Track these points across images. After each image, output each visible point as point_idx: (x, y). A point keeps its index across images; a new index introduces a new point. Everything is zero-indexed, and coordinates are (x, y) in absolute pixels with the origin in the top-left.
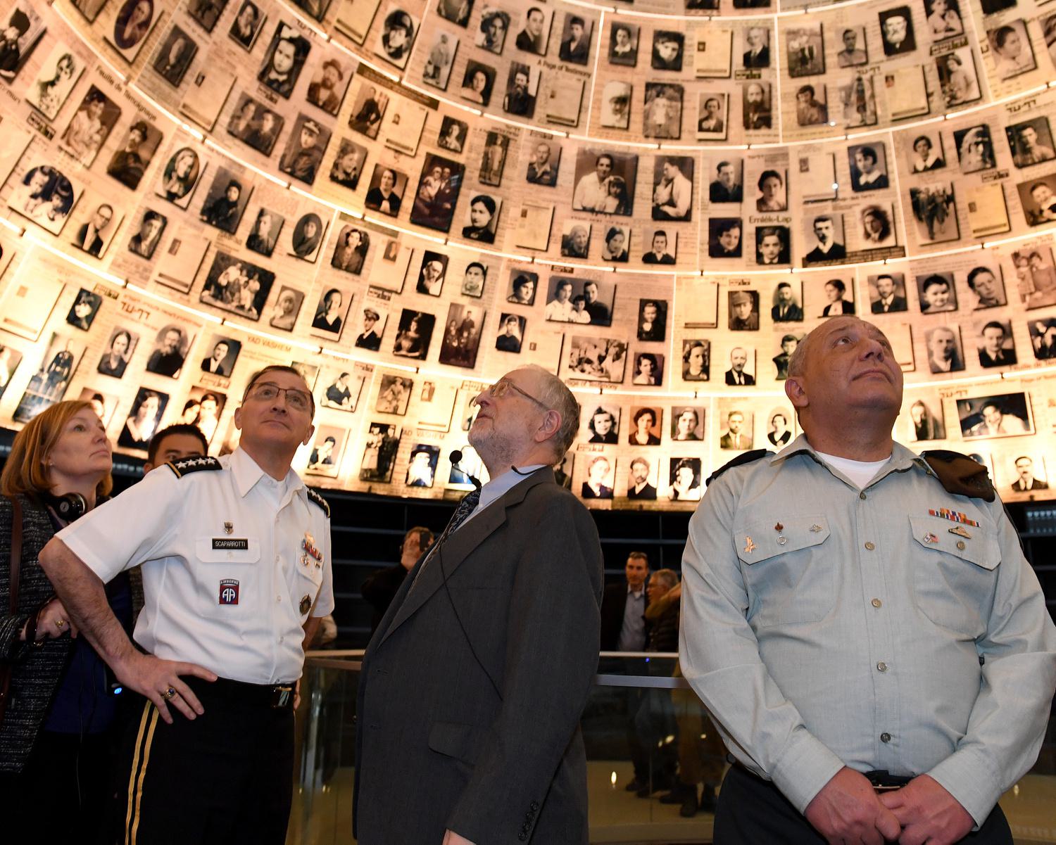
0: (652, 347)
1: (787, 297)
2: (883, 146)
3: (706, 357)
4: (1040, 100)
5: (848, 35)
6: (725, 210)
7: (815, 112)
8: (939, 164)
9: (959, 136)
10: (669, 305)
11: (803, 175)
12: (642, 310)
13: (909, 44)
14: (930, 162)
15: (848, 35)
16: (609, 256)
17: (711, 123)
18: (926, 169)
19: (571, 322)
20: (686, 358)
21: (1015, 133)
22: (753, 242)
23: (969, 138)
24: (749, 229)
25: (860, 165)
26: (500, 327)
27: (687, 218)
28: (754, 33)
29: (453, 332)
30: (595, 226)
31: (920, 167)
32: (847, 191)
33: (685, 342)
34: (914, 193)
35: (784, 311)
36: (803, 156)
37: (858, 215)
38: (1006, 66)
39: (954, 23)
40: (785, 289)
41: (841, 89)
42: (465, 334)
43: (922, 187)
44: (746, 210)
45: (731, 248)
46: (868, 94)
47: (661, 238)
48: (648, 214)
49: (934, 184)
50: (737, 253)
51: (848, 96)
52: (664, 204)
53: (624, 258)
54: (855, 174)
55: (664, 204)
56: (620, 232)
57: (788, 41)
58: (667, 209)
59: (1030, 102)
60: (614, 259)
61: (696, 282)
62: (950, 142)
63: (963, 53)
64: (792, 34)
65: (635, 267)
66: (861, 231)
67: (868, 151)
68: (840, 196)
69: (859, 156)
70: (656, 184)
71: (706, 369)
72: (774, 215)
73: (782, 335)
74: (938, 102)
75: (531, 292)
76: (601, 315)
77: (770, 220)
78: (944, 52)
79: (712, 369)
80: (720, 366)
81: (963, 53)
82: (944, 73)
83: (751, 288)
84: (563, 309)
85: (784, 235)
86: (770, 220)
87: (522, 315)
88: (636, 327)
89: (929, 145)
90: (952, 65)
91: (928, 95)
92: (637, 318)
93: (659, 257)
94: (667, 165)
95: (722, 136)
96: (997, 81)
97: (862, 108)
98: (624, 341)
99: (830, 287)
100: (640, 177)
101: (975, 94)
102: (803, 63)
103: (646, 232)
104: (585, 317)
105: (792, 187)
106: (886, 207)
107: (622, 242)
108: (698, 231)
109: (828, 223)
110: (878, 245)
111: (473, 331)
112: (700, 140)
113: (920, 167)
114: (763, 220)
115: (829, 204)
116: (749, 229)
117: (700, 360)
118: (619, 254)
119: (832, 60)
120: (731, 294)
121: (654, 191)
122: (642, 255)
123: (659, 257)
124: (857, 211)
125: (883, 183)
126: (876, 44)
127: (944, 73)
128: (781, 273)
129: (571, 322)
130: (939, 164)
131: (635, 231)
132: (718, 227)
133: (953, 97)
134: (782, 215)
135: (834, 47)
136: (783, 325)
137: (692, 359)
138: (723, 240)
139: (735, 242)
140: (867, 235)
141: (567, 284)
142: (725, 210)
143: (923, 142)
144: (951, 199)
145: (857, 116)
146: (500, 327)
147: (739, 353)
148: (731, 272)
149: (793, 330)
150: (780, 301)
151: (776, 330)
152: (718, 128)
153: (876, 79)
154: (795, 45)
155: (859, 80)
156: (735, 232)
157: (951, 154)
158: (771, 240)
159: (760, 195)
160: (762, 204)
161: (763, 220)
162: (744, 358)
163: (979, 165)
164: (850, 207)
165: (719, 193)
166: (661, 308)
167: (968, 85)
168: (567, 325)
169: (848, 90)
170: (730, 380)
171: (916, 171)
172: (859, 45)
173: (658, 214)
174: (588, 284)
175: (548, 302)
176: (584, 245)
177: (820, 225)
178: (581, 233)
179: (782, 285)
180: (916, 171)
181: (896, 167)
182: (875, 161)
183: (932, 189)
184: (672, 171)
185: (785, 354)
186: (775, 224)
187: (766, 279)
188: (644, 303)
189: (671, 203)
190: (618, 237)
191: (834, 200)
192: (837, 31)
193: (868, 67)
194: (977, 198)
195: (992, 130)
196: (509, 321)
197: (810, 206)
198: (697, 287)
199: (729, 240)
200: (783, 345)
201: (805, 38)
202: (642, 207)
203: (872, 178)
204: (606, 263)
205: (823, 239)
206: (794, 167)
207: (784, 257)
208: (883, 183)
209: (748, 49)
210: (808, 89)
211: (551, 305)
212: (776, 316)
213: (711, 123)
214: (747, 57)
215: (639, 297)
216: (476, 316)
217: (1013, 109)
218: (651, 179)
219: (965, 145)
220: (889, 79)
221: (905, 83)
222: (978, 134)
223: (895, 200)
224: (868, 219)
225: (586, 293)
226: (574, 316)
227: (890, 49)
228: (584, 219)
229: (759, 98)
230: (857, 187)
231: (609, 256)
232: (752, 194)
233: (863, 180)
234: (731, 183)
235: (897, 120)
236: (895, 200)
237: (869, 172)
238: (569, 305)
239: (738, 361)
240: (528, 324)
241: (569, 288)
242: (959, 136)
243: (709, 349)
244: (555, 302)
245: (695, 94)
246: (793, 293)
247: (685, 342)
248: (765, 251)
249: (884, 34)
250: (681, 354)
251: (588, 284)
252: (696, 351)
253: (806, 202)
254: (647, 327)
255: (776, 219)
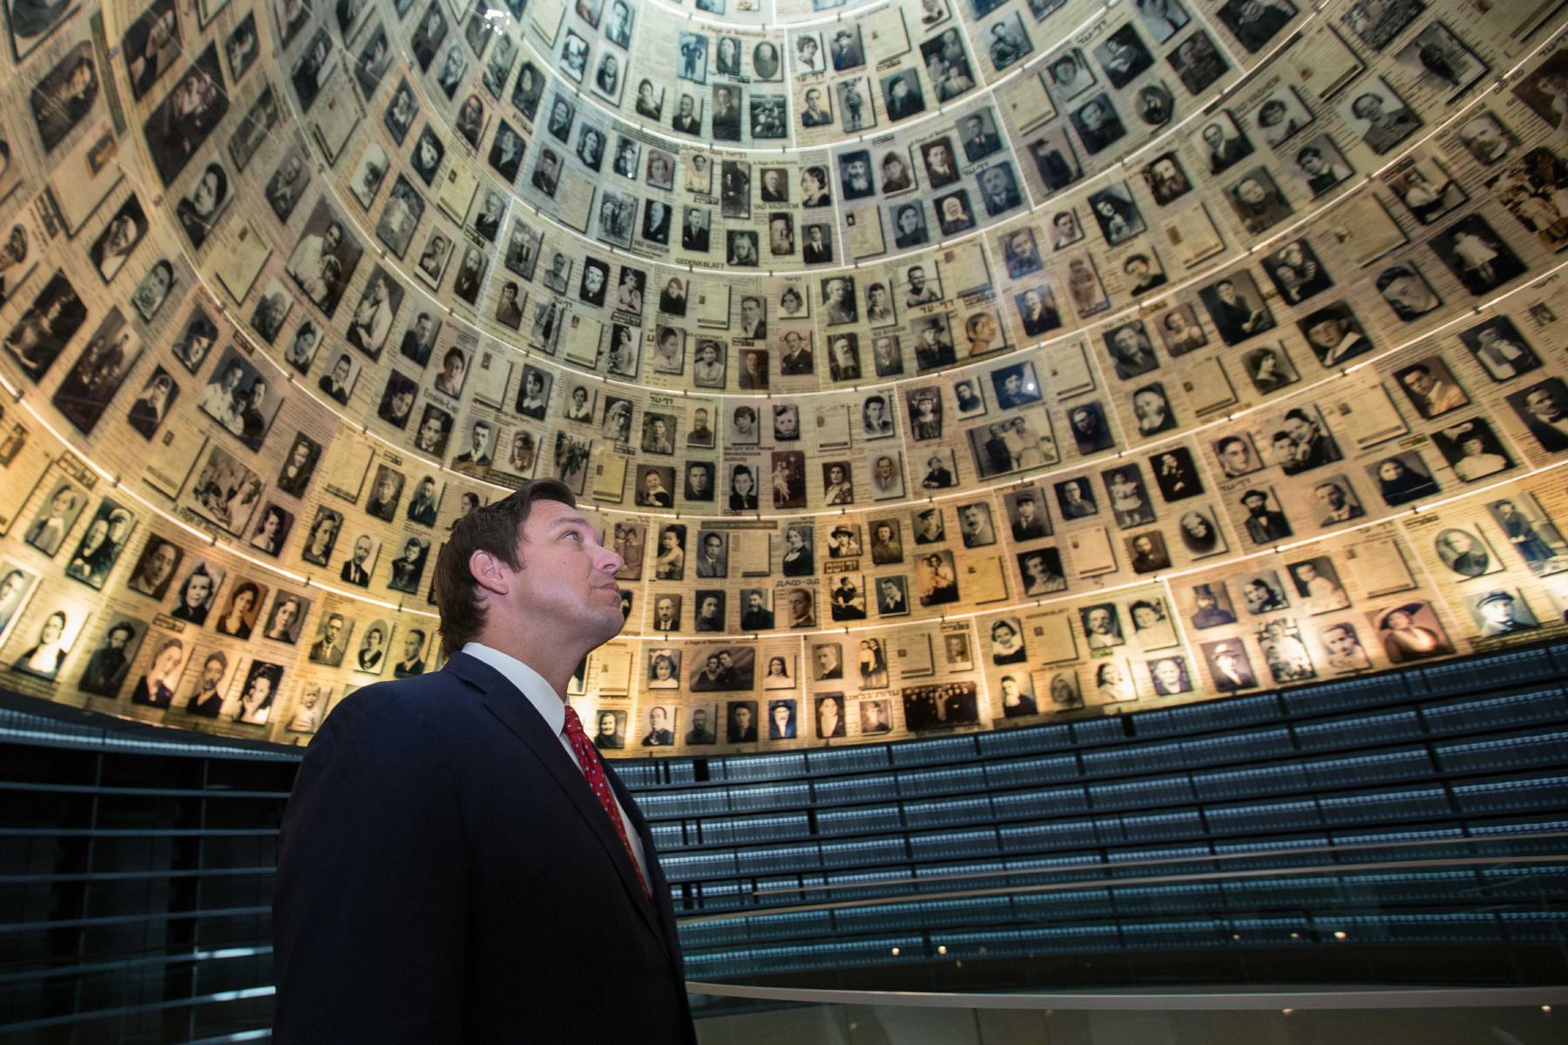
0: (286, 501)
1: (428, 494)
2: (552, 379)
3: (333, 535)
4: (677, 402)
5: (558, 259)
6: (409, 369)
7: (510, 316)
8: (587, 419)
9: (610, 402)
10: (324, 453)
11: (483, 371)
12: (295, 448)
13: (598, 299)
14: (581, 414)
15: (558, 259)
16: (292, 357)
17: (431, 264)
18: (576, 419)
19: (221, 424)
20: (315, 529)
21: (652, 419)
22: (419, 418)
23: (616, 408)
24: (422, 401)
25: (529, 387)
26: (147, 387)
27: (374, 355)
28: (494, 199)
29: (93, 358)
30: (297, 308)
31: (573, 415)
32: (510, 407)
33: (321, 508)
34: (561, 436)
35: (420, 509)
36: (490, 351)
37: (512, 437)
38: (661, 361)
39: (637, 303)
40: (429, 486)
41: (538, 305)
42: (105, 371)
43: (568, 434)
44: (425, 378)
45: (399, 414)
46: (555, 323)
47: (344, 365)
48: (344, 330)
49: (578, 436)
50: (400, 423)
51: (541, 316)
52: (362, 326)
53: (303, 369)
54: (522, 394)
55: (362, 326)
56: (313, 333)
57: (515, 230)
58: (362, 332)
59: (669, 399)
60: (295, 364)
61: (357, 438)
62: (601, 404)
63: (635, 332)
64: (520, 225)
65: (308, 387)
66: (508, 454)
67: (540, 378)
68: (505, 409)
69: (530, 378)
70: (365, 297)
71: (327, 551)
72: (446, 399)
73: (411, 535)
74: (604, 364)
75: (201, 352)
76: (254, 432)
77: (442, 402)
78: (621, 323)
79: (334, 553)
80: (344, 552)
81: (635, 332)
82: (616, 343)
83: (401, 469)
84: (219, 401)
85: (447, 424)
86: (442, 402)
87: (179, 382)
88: (280, 466)
89: (585, 397)
90: (624, 339)
91: (600, 353)
92: (286, 454)
93: (335, 388)
94: (381, 282)
95: (434, 284)
96: (651, 369)
97: (546, 334)
98: (263, 481)
99: (467, 500)
100: (356, 278)
101: (632, 372)
102: (518, 259)
103: (335, 347)
104: (238, 425)
105: (471, 379)
106: (536, 439)
107: (310, 345)
108: (375, 378)
109: (486, 432)
110: (517, 473)
111: (117, 371)
112: (417, 276)
113: (573, 415)
114: (435, 399)
115: (493, 411)
116: (422, 401)
117: (327, 537)
118: (301, 361)
119: (540, 273)
120: (381, 467)
121: (360, 304)
122: (321, 374)
123: (335, 388)
124: (514, 430)
125: (539, 414)
126: (576, 282)
127: (616, 343)
128: (430, 465)
129: (221, 424)
130: (587, 419)
131: (327, 339)
132: (399, 385)
133: (615, 365)
134: (453, 403)
135: (544, 264)
136: (415, 525)
137: (320, 534)
138: (396, 402)
139: (405, 409)
140: (512, 460)
141: (239, 366)
142: (409, 369)
143: (581, 393)
144: (586, 455)
145: (541, 338)
146: (147, 387)
147: (364, 543)
148: (391, 442)
149: (421, 533)
150: (420, 497)
151: (407, 528)
152: (434, 274)
153: (566, 313)
154: (519, 237)
155: (554, 306)
156: (408, 398)
157: (599, 415)
158: (435, 424)
159: (442, 370)
160: (441, 380)
161: (435, 399)
162: (367, 551)
163: (616, 435)
164: (508, 424)
165: (414, 348)
166: (315, 453)
167: (630, 361)
168: (217, 427)
169: (543, 308)
170: (345, 576)
171: (568, 417)
172: (564, 274)
173: (353, 336)
174: (259, 380)
175: (212, 381)
176: (276, 324)
177: (479, 430)
178: (280, 307)
179: (429, 480)
180: (568, 417)
181: (557, 402)
182: (540, 391)
183: (575, 440)
184: (383, 292)
185: (404, 560)
186: (444, 408)
187: (418, 466)
188: (301, 438)
189: (369, 328)
190: (309, 336)
191: (499, 410)
192: (553, 249)
193: (563, 299)
194: (605, 462)
195: (635, 409)
196: (162, 382)
197: (478, 406)
198: (356, 447)
199: (400, 406)
200: (407, 549)
201: (527, 237)
202: (343, 317)
203: (534, 404)
204: (284, 363)
205: (477, 445)
206: (478, 359)
207: (439, 450)
208: (539, 414)
209: (484, 211)
210: (512, 286)
211: (211, 387)
212: (412, 515)
213: (431, 264)
214: (481, 217)
215: (298, 428)
216: (129, 349)
217: (655, 398)
218: (363, 287)
219: (611, 412)
220: (576, 320)
221: (585, 332)
222: (623, 407)
223: (544, 434)
224: (519, 443)
225: (253, 392)
226: (228, 416)
227: (584, 294)
228: (290, 290)
229: (475, 267)
230: (520, 408)
231: (292, 357)
232: (435, 367)
233: (527, 403)
234: (424, 342)
235: (570, 361)
236: (544, 434)
237: (533, 398)
238: (229, 398)
239: (361, 552)
240: (179, 400)
241: (239, 373)
242: (610, 402)
243: (338, 528)
244: (218, 386)
245: (432, 221)
246: (435, 489)
247: (321, 508)
248: (428, 434)
249: (585, 278)
250: (311, 522)
251: (259, 380)
252: (327, 524)
253: (476, 400)
254: (292, 472)
255: (446, 404)
